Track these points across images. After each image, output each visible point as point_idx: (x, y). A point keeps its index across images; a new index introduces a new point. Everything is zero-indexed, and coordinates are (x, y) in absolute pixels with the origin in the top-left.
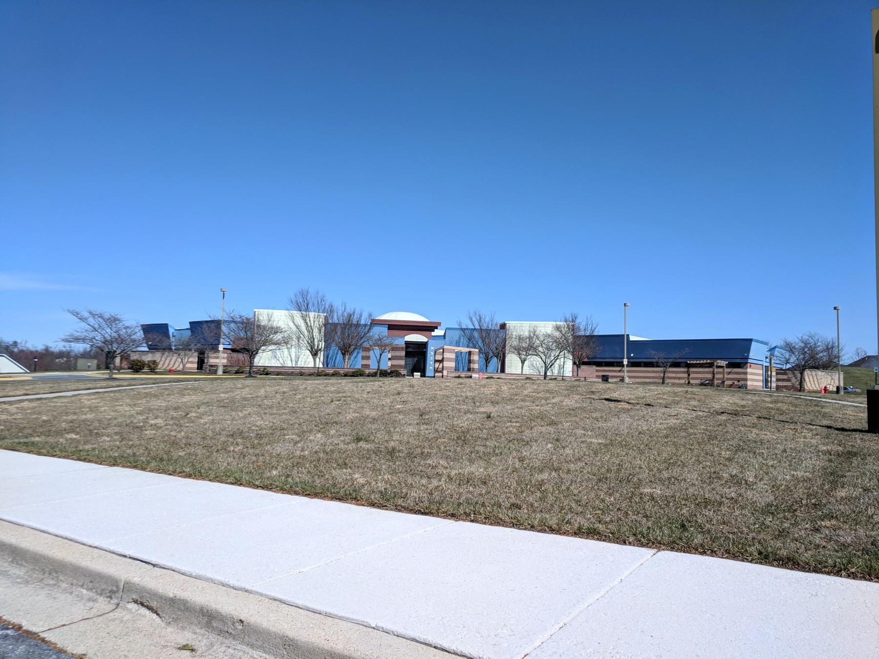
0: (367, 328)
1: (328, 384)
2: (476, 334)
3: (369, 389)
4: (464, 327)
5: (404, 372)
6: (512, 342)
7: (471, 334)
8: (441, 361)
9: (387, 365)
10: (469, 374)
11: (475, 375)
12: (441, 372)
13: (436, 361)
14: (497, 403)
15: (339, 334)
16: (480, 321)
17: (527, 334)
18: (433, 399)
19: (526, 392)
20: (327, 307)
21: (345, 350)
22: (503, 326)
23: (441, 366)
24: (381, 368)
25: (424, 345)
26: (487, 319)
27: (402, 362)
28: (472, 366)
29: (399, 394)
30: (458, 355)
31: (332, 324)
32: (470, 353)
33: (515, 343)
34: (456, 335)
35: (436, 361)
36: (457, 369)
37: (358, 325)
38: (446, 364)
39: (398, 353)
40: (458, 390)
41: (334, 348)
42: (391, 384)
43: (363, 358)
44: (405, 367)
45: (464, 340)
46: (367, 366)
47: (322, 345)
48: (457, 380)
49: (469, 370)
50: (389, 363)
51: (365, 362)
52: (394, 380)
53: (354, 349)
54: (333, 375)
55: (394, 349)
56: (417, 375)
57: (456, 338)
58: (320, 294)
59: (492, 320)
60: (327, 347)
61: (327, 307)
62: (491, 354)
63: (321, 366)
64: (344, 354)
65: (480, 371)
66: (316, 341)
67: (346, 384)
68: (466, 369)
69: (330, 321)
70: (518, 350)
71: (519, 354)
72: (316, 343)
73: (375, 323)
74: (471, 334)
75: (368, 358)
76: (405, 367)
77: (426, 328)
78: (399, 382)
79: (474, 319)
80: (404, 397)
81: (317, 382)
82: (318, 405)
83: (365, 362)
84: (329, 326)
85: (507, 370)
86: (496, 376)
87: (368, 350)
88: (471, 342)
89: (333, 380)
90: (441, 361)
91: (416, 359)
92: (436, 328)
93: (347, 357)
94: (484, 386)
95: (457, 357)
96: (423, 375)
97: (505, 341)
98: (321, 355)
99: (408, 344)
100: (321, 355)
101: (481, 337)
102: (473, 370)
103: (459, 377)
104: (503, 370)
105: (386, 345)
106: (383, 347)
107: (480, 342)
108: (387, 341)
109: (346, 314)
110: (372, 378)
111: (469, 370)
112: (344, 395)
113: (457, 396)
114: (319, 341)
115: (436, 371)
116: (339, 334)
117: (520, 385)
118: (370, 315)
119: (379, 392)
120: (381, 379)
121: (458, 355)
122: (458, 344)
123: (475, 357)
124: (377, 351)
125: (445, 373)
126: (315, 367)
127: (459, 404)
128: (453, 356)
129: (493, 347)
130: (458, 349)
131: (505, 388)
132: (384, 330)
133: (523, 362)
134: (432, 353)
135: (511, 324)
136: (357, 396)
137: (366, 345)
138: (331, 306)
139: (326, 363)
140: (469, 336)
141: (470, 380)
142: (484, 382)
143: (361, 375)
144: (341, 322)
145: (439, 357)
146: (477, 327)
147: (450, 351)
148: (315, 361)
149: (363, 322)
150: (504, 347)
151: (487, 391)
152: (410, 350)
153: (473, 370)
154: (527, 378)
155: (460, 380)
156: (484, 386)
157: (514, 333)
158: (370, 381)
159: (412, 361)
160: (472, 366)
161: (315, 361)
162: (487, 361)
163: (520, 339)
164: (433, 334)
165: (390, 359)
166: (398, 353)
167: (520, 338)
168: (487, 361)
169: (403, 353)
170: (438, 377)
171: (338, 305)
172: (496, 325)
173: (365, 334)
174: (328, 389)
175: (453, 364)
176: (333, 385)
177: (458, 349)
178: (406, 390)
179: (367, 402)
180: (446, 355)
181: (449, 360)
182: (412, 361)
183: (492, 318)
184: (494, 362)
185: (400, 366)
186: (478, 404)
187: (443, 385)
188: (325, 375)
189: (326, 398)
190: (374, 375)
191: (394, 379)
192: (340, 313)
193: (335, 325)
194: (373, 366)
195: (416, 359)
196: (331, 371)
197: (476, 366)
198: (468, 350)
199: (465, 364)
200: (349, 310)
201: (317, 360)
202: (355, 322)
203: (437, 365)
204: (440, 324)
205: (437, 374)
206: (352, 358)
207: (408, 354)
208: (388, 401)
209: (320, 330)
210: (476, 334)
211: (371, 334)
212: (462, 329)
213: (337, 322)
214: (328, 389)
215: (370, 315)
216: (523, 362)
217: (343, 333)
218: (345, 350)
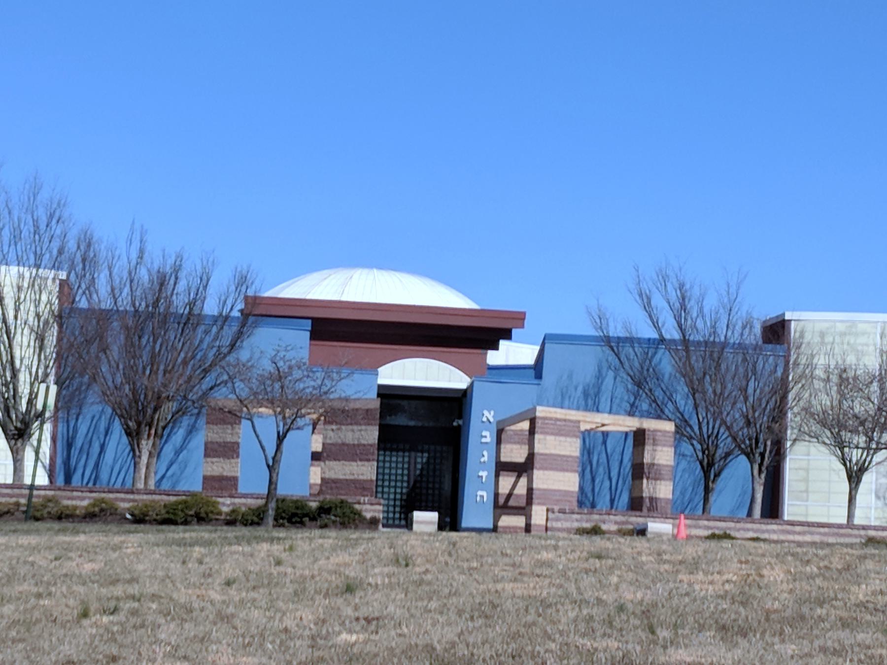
0: (229, 332)
1: (68, 548)
2: (666, 363)
3: (230, 570)
4: (616, 330)
5: (372, 509)
6: (811, 396)
7: (647, 358)
8: (524, 469)
9: (303, 480)
10: (636, 520)
11: (657, 527)
12: (524, 510)
13: (502, 467)
14: (744, 633)
15: (115, 352)
16: (682, 309)
17: (872, 363)
18: (487, 611)
19: (860, 593)
20: (72, 245)
21: (141, 419)
22: (776, 331)
23: (521, 489)
24: (282, 490)
25: (455, 404)
26: (711, 303)
27: (367, 471)
28: (648, 488)
29: (349, 589)
30: (593, 443)
31: (90, 312)
32: (640, 437)
33: (824, 400)
34: (586, 363)
35: (502, 467)
36: (586, 500)
37: (191, 320)
38: (542, 479)
39: (351, 435)
40: (588, 581)
41: (95, 410)
42: (319, 553)
43: (212, 450)
44: (378, 488)
45: (615, 386)
46: (227, 484)
47: (48, 395)
48: (585, 541)
49: (636, 504)
50: (316, 474)
51: (219, 467)
52: (329, 538)
53: (180, 412)
54: (91, 516)
55: (338, 415)
56: (426, 519)
57: (585, 373)
58: (44, 195)
59: (734, 301)
60: (69, 402)
61: (72, 245)
62: (725, 443)
63: (42, 479)
64: (134, 436)
65: (678, 509)
66: (24, 379)
67: (143, 553)
68: (625, 498)
69: (83, 304)
70: (837, 428)
71: (841, 445)
72: (24, 390)
73: (260, 312)
74: (647, 358)
75: (230, 450)
76: (378, 488)
77: (469, 336)
78: (356, 543)
79: (658, 301)
80: (373, 603)
81: (24, 540)
82: (29, 625)
83: (219, 467)
84: (75, 322)
85: (791, 509)
86: (745, 530)
87: (230, 417)
88: (645, 392)
89: (88, 537)
90: (524, 469)
91: (421, 459)
92: (506, 334)
93: (146, 445)
94: (694, 566)
95: (587, 451)
96: (450, 520)
97: (782, 389)
98: (44, 437)
99: (392, 398)
100: (44, 437)
101: (686, 372)
102: (654, 507)
103: (595, 531)
104: (772, 508)
105: (300, 402)
106: (291, 409)
107: (682, 389)
108: (308, 386)
109: (143, 275)
110: (245, 531)
111: (636, 504)
112: (134, 589)
113: (581, 603)
114: (36, 380)
115: (502, 506)
116: (115, 352)
117: (837, 563)
118: (242, 281)
119: (270, 583)
120: (281, 533)
121: (593, 443)
122: (591, 401)
123: (662, 455)
124: (267, 422)
125: (539, 515)
126: (18, 484)
127: (590, 633)
128: (571, 448)
129: (735, 415)
130: (590, 420)
131: (775, 574)
132: (296, 341)
133: (855, 476)
134: (488, 437)
135: (809, 323)
136: (182, 595)
137: (223, 398)
138: (87, 243)
139: (64, 469)
140: (635, 369)
141: (639, 543)
142: (690, 551)
143: (201, 519)
144: (124, 302)
145: (515, 453)
146: (672, 332)
147: (562, 429)
148: (18, 462)
149: (211, 308)
150: (779, 413)
151: (705, 586)
152: (401, 420)
153: (654, 507)
154: (871, 541)
155: (598, 542)
156: (694, 566)
157: (821, 361)
158: (238, 540)
159: (406, 465)
160: (648, 488)
161: (18, 462)
162: (710, 469)
163: (843, 380)
164: (494, 358)
165: (316, 457)
166: (351, 435)
167: (846, 382)
168: (710, 469)
169: (371, 435)
170: (512, 530)
171: (113, 235)
172: (748, 324)
173: (220, 356)
174: (70, 566)
175: (568, 482)
176: (87, 551)
177: (590, 420)
178: (378, 574)
179: (223, 618)
180: (545, 444)
181: (557, 463)
182: (406, 465)
183: (734, 292)
184: (739, 476)
185: (359, 486)
186: (663, 634)
187: (526, 561)
188: (60, 518)
189: (62, 603)
190: (252, 519)
191: (332, 533)
192: (121, 269)
193: (103, 317)
194: (252, 483)
195: (421, 459)
196: (83, 502)
197: (664, 490)
198: (631, 424)
199: (617, 482)
200: (158, 256)
201: (29, 455)
202: (179, 303)
203: (506, 482)
204: (519, 318)
205: (506, 521)
206: (168, 450)
207: (390, 440)
208: (308, 616)
209: (41, 339)
210: (666, 363)
211: (244, 355)
212: (608, 341)
213: (107, 304)
214: (70, 566)
215: (242, 281)
216: (855, 476)
217: (131, 349)
218: (141, 419)
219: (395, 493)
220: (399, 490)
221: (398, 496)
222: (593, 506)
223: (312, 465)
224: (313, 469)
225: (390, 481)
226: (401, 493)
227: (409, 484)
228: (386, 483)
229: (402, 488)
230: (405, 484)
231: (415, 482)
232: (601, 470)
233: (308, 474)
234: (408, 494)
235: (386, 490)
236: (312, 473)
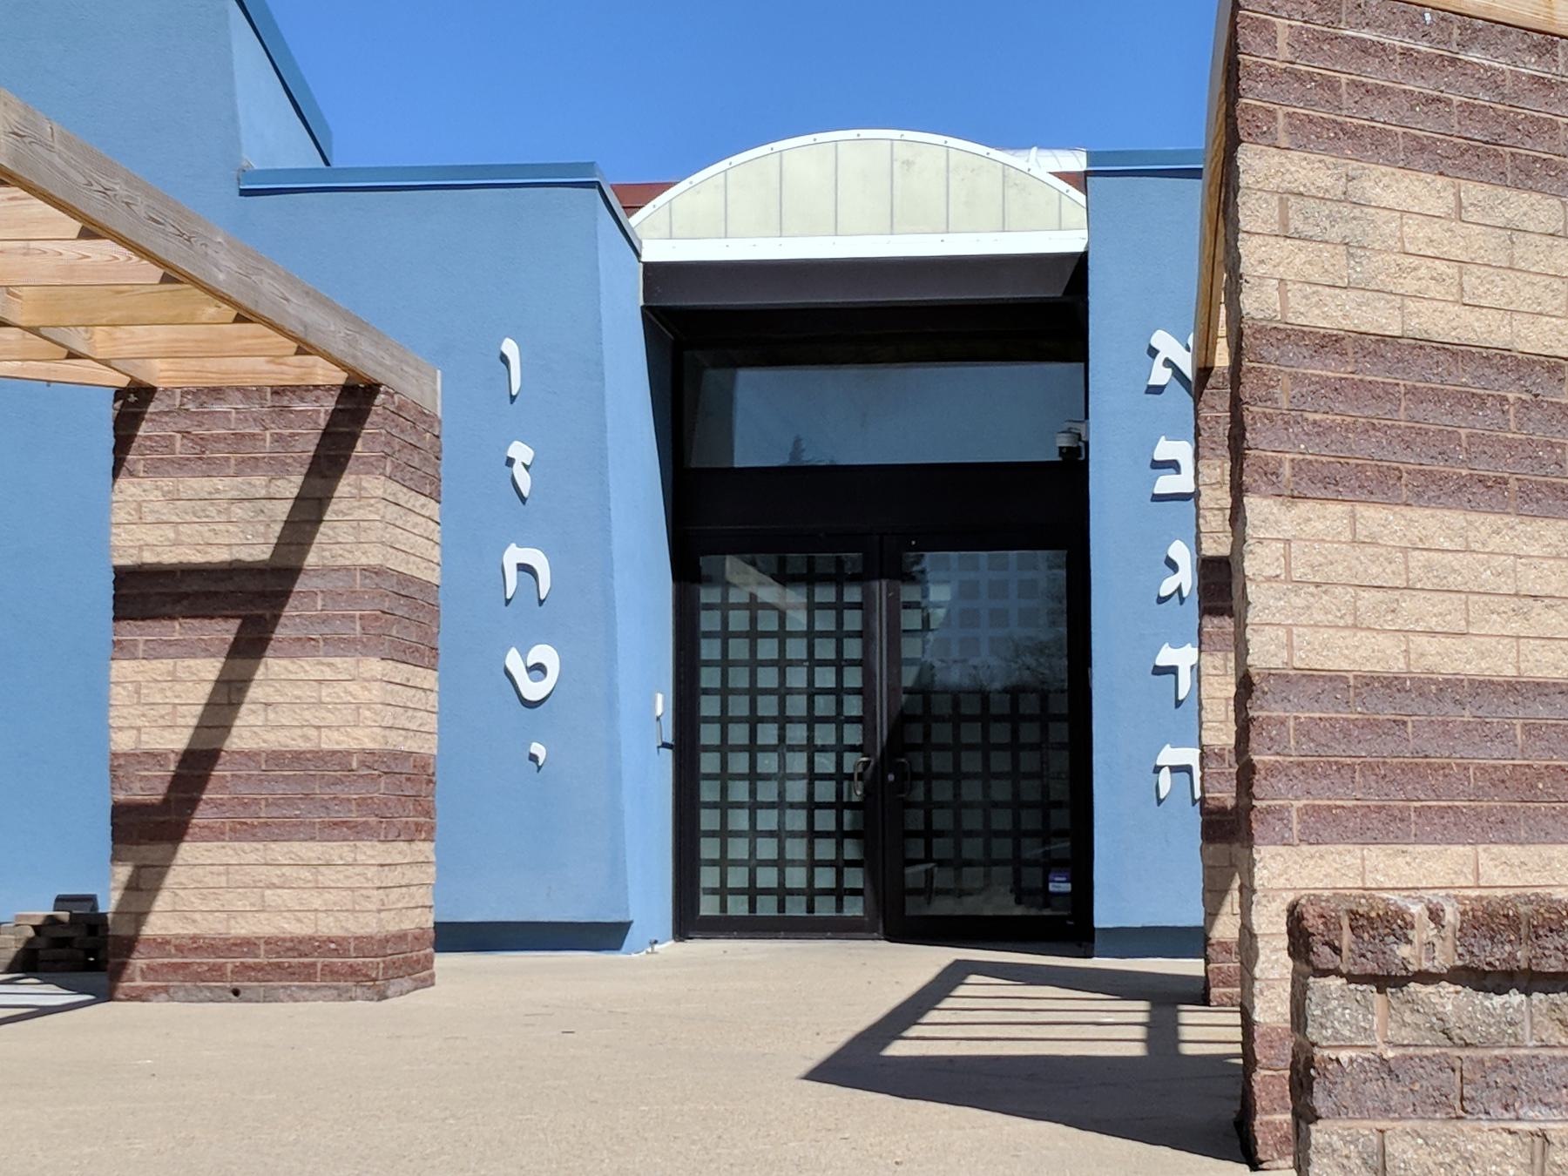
219: (812, 777)
220: (825, 763)
221: (826, 791)
223: (121, 649)
224: (122, 669)
225: (754, 721)
226: (839, 777)
227: (869, 732)
228: (767, 735)
229: (840, 749)
230: (853, 735)
231: (901, 721)
233: (97, 701)
234: (874, 782)
235: (768, 763)
236: (119, 695)
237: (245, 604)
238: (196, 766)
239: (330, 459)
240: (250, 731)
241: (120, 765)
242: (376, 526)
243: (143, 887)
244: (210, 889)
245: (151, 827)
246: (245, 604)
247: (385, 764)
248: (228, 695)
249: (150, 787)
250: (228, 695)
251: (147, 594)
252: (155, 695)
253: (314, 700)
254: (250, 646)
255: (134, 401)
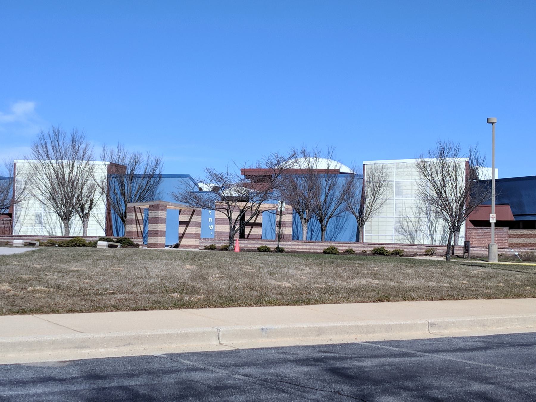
222: (298, 239)
232: (299, 224)
237: (187, 224)
238: (184, 234)
239: (192, 214)
240: (187, 232)
241: (179, 234)
242: (195, 219)
243: (180, 241)
244: (184, 242)
245: (181, 238)
246: (187, 224)
247: (196, 234)
248: (186, 229)
249: (181, 235)
250: (186, 229)
251: (181, 223)
252: (181, 229)
253: (191, 230)
254: (187, 226)
255: (180, 211)
